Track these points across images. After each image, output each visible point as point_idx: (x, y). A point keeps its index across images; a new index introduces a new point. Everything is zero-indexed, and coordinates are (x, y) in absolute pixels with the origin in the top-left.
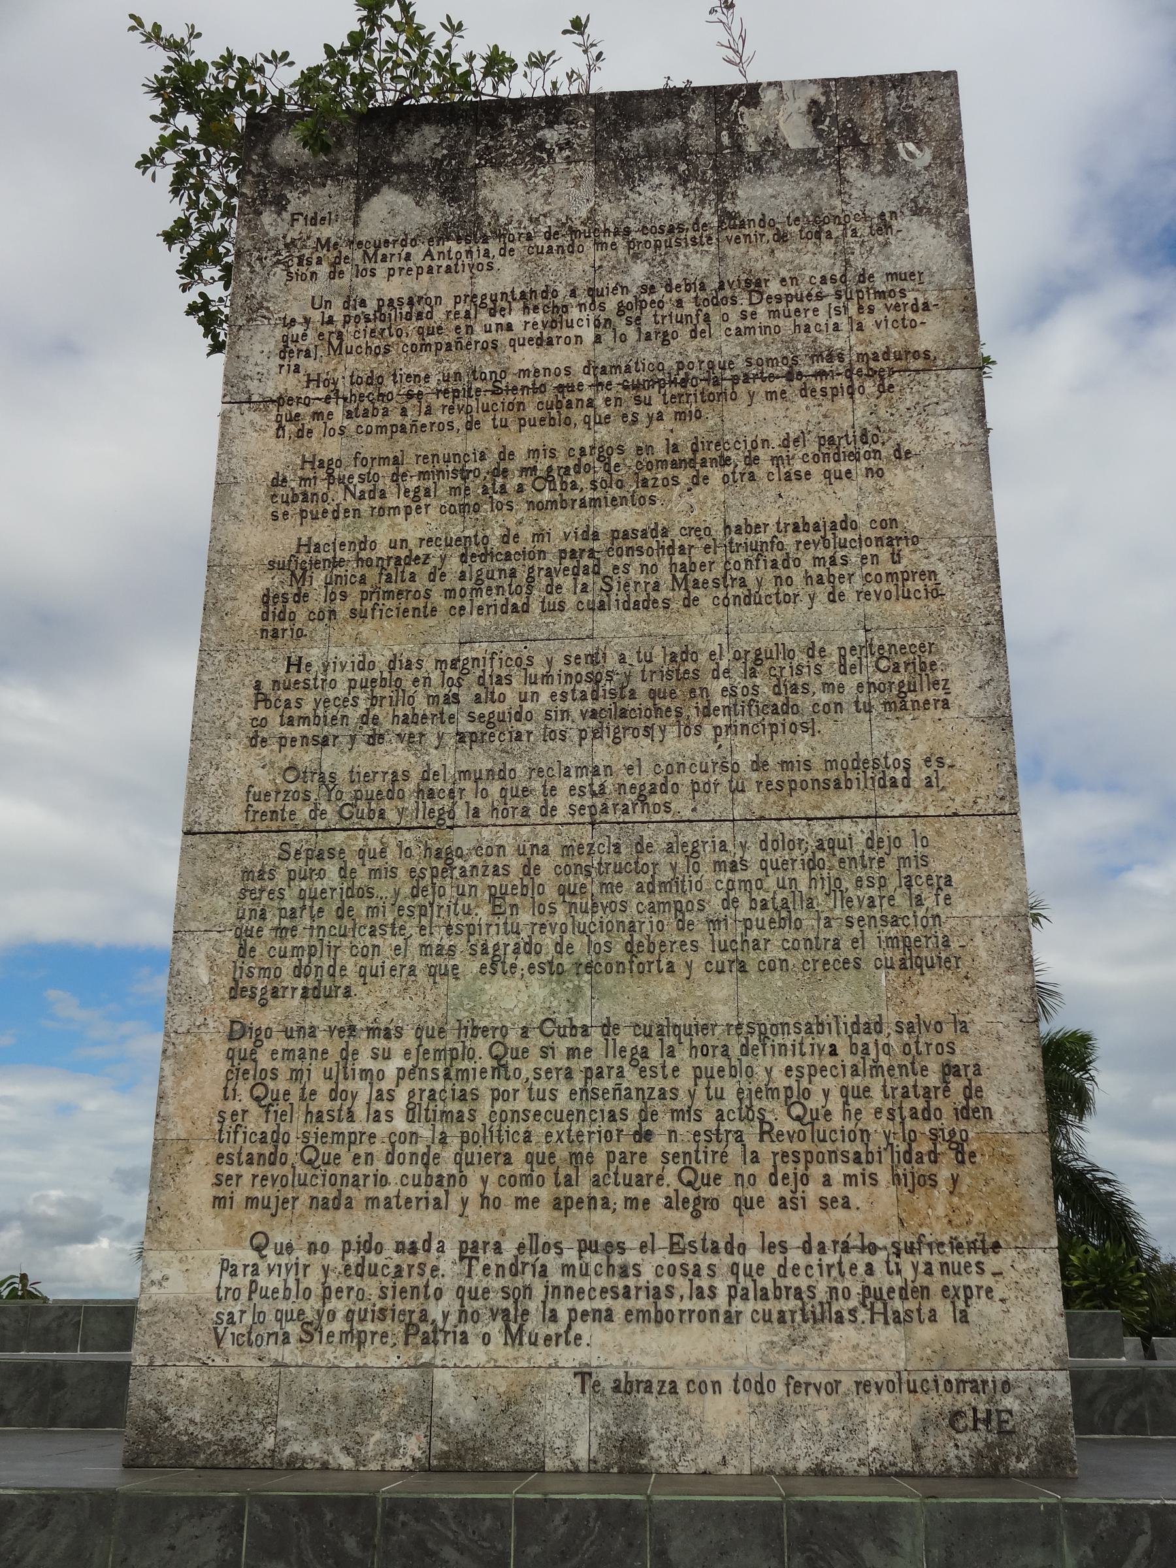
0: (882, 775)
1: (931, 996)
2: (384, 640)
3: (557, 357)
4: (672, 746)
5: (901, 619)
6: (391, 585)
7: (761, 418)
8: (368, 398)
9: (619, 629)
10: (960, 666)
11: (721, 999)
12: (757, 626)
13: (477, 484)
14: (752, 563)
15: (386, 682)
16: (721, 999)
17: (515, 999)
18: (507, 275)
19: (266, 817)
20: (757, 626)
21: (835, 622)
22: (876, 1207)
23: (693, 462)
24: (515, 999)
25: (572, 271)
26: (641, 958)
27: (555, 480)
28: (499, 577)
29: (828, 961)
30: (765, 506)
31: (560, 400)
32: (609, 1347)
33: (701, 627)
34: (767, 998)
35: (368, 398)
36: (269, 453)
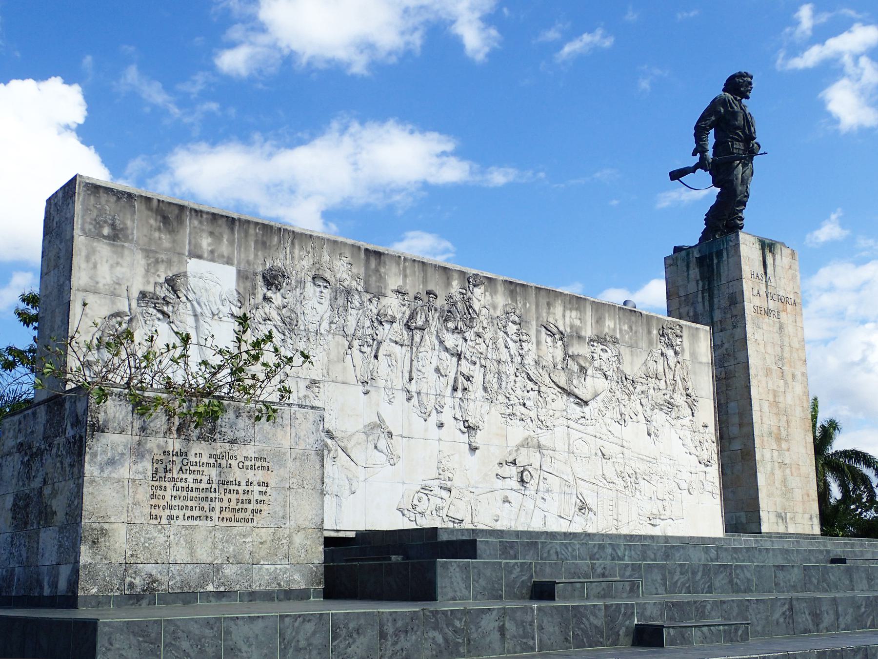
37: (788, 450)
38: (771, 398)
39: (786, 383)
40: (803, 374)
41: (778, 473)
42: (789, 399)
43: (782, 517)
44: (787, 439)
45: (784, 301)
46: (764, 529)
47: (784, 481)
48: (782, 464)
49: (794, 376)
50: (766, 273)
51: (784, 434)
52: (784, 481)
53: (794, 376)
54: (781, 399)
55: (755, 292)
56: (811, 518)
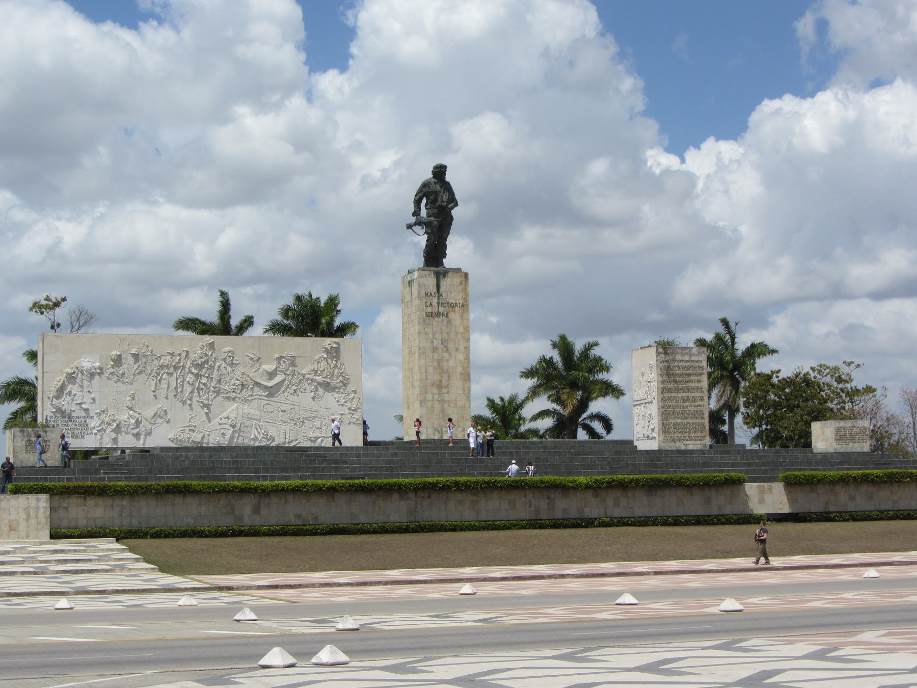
2: (669, 394)
5: (701, 395)
6: (669, 390)
7: (693, 378)
9: (684, 394)
11: (691, 421)
12: (693, 395)
13: (675, 381)
14: (693, 390)
15: (669, 398)
16: (691, 421)
17: (679, 421)
19: (663, 407)
20: (693, 395)
21: (697, 394)
24: (679, 421)
25: (680, 364)
28: (677, 390)
30: (693, 385)
32: (686, 442)
33: (690, 395)
34: (694, 421)
36: (661, 379)
38: (436, 364)
39: (450, 354)
40: (466, 347)
41: (437, 407)
42: (451, 363)
44: (447, 387)
45: (452, 306)
48: (442, 402)
49: (457, 349)
51: (444, 384)
54: (444, 364)
55: (428, 304)
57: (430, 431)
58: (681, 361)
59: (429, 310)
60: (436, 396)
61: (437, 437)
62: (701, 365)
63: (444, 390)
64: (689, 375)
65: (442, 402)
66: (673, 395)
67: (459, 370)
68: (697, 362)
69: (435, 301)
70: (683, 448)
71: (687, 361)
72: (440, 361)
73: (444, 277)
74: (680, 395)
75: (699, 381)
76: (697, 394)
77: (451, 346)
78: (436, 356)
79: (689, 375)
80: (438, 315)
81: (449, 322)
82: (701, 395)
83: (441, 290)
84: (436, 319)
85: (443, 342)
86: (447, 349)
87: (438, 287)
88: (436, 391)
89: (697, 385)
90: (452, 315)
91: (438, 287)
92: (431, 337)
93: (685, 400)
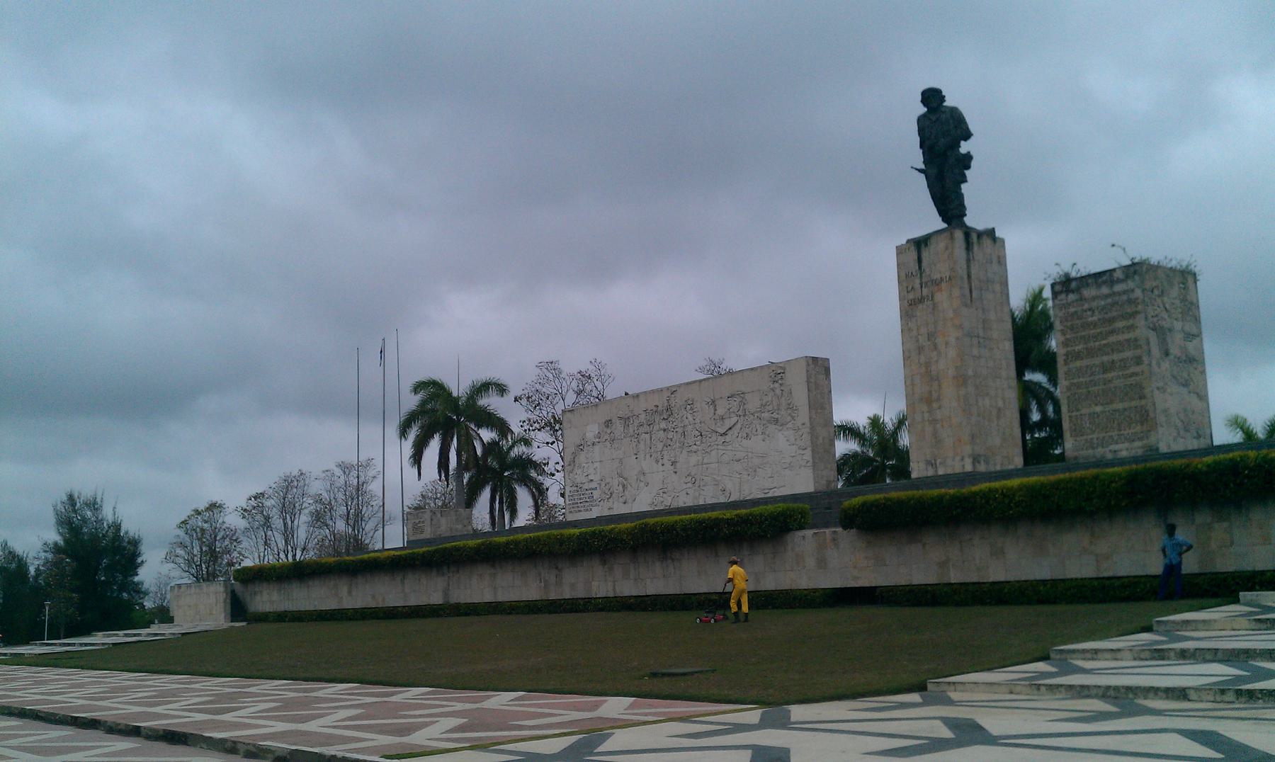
0: (1136, 374)
1: (1143, 402)
2: (1078, 364)
3: (1095, 318)
4: (1113, 374)
5: (1138, 352)
6: (1078, 356)
7: (1120, 324)
8: (1072, 328)
9: (1105, 358)
10: (1145, 359)
11: (1120, 406)
15: (1079, 369)
17: (1098, 409)
18: (1086, 306)
21: (1128, 354)
22: (1138, 428)
23: (1112, 332)
24: (1098, 409)
25: (1094, 304)
26: (1111, 402)
27: (1095, 337)
28: (1091, 353)
29: (1132, 399)
30: (1121, 337)
31: (1095, 325)
33: (1116, 357)
34: (1126, 405)
35: (1072, 328)
37: (940, 408)
38: (923, 369)
41: (929, 429)
43: (930, 463)
44: (938, 399)
45: (937, 283)
46: (914, 475)
47: (935, 434)
48: (934, 422)
49: (947, 344)
50: (920, 267)
51: (935, 395)
52: (935, 434)
53: (947, 344)
54: (933, 368)
56: (962, 459)
57: (922, 465)
58: (1094, 298)
59: (911, 296)
60: (926, 415)
61: (930, 473)
62: (1132, 296)
63: (935, 405)
64: (1113, 320)
65: (934, 422)
66: (1086, 362)
67: (951, 372)
68: (1125, 292)
69: (918, 281)
70: (1110, 456)
71: (1107, 296)
72: (928, 365)
73: (926, 245)
74: (1097, 361)
75: (1131, 328)
76: (1128, 354)
77: (939, 340)
78: (923, 359)
79: (1113, 320)
80: (921, 300)
81: (935, 307)
82: (1138, 352)
83: (924, 264)
84: (920, 306)
85: (930, 336)
86: (935, 347)
87: (920, 261)
88: (925, 408)
89: (1126, 336)
90: (938, 297)
91: (920, 261)
92: (915, 333)
93: (1106, 369)
